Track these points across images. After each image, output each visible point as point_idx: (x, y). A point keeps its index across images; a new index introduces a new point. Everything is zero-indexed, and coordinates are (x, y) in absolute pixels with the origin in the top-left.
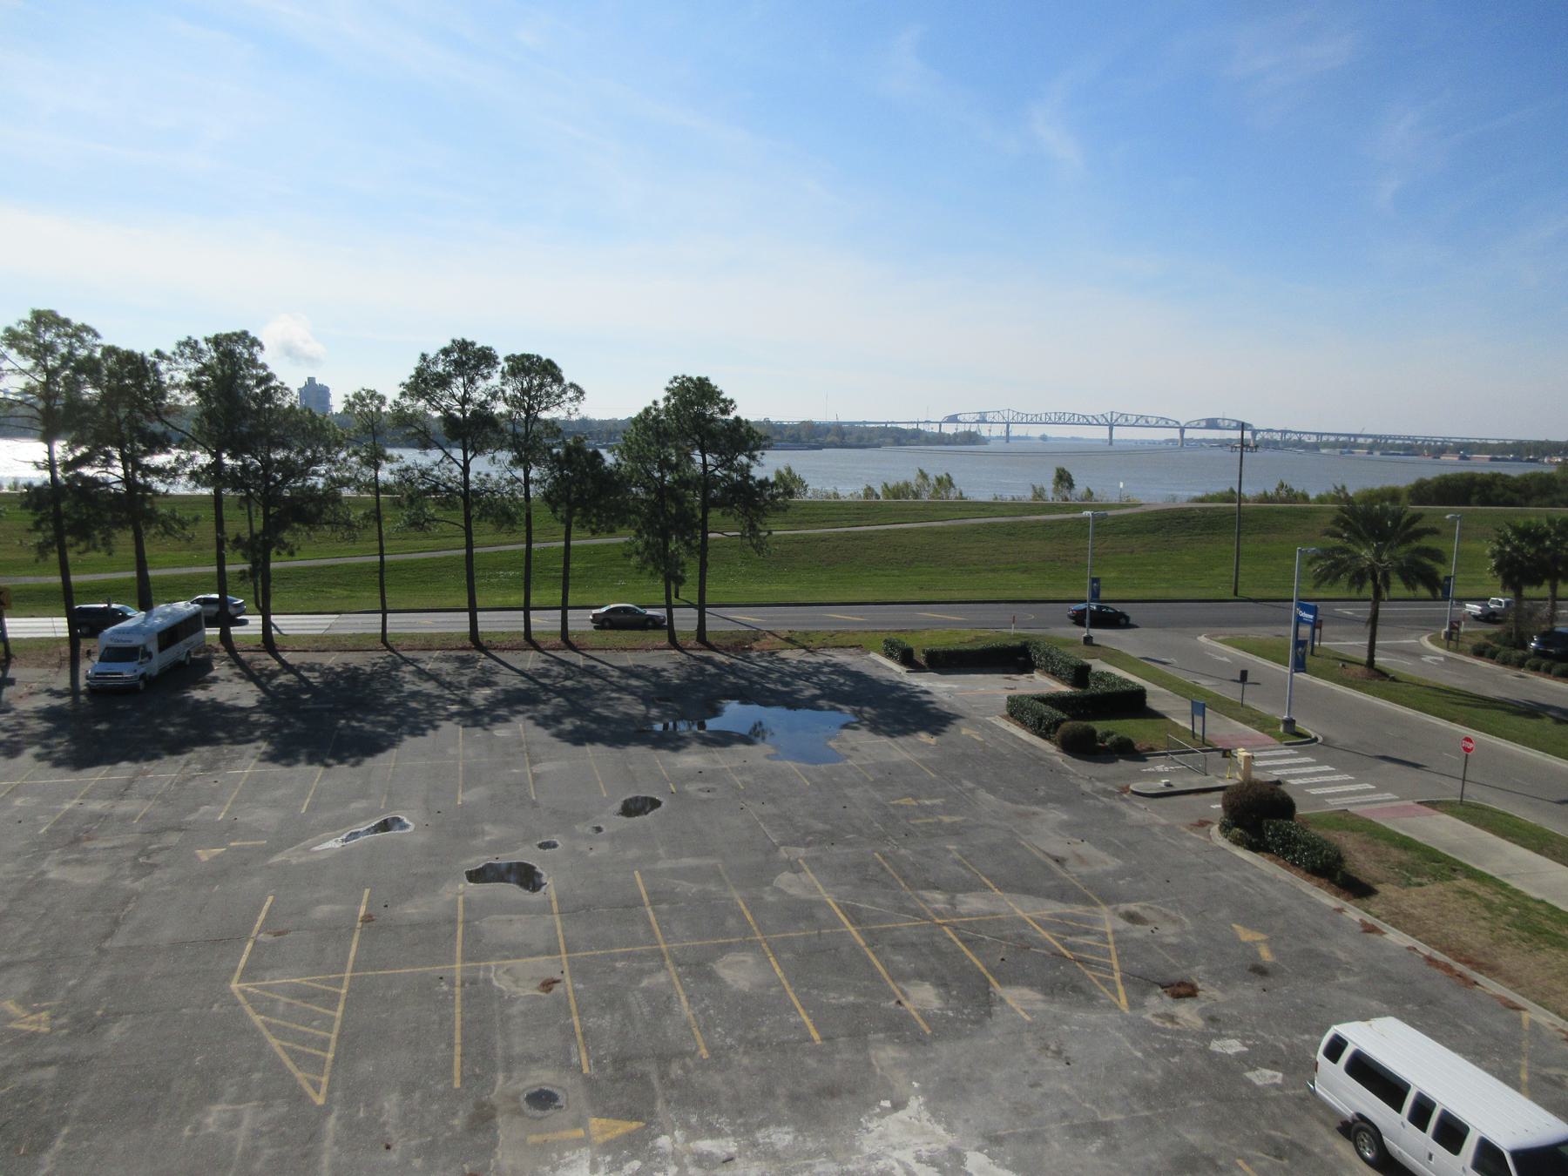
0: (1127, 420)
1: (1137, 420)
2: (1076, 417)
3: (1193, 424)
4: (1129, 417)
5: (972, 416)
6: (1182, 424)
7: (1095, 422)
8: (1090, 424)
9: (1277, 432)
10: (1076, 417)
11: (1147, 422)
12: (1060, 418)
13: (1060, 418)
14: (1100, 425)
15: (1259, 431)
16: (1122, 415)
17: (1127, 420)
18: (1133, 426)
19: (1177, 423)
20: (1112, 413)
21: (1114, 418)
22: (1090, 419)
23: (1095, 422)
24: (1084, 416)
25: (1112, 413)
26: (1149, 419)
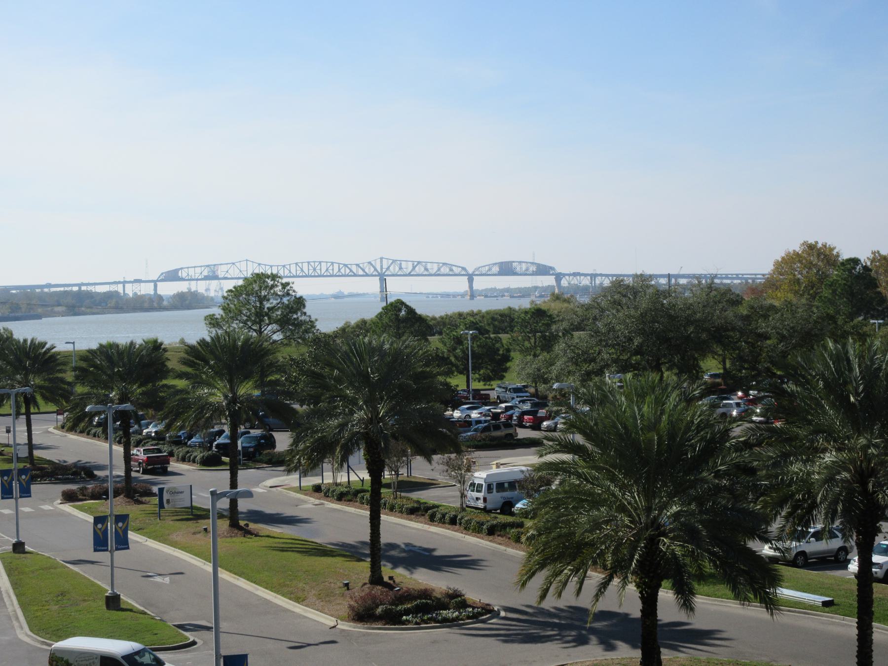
0: (401, 268)
1: (414, 268)
2: (336, 266)
3: (484, 270)
4: (404, 265)
5: (198, 270)
6: (470, 272)
7: (361, 272)
8: (355, 275)
9: (585, 275)
10: (336, 266)
11: (426, 269)
12: (315, 269)
13: (315, 269)
14: (367, 275)
15: (564, 275)
16: (394, 261)
17: (401, 268)
18: (409, 275)
19: (464, 269)
20: (381, 259)
21: (385, 266)
22: (354, 268)
23: (361, 272)
24: (346, 265)
25: (381, 259)
26: (429, 266)
